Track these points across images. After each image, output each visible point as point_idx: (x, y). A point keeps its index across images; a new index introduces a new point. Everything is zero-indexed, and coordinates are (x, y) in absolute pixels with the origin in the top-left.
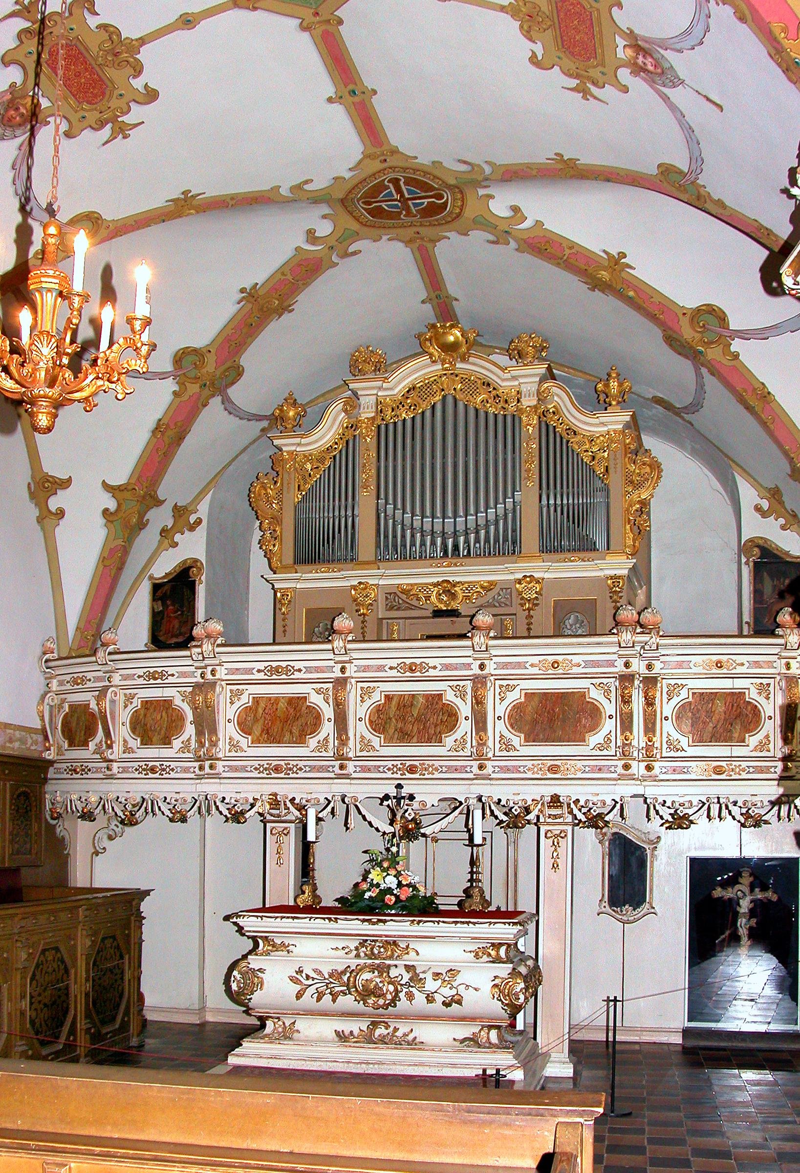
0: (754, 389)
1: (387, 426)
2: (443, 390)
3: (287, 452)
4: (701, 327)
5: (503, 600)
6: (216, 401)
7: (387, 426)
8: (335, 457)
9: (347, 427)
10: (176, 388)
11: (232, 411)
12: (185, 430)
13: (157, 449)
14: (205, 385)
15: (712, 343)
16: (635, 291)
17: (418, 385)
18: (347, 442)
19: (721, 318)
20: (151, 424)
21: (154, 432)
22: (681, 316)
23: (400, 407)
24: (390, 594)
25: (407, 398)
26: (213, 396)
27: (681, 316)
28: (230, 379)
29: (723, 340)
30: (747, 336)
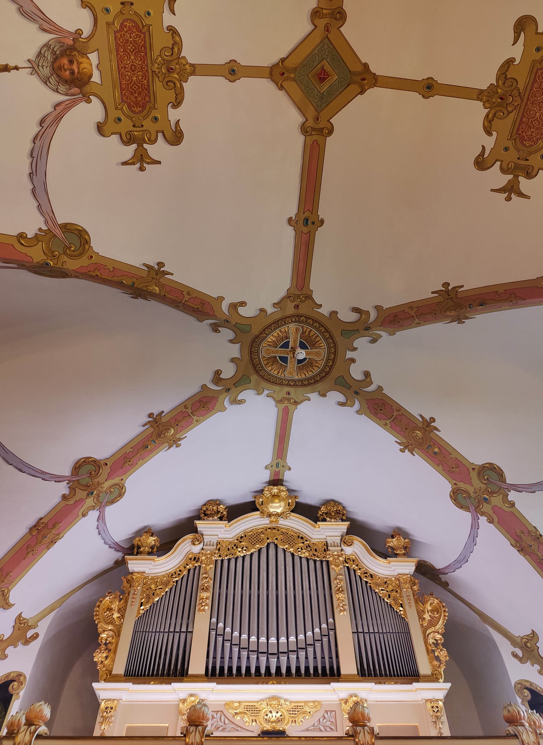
0: (529, 532)
1: (222, 561)
2: (268, 539)
3: (138, 573)
4: (485, 480)
5: (328, 724)
6: (94, 515)
7: (222, 561)
8: (177, 581)
9: (191, 559)
10: (66, 491)
11: (102, 532)
12: (59, 534)
13: (28, 546)
14: (92, 493)
15: (495, 493)
16: (439, 448)
17: (250, 534)
18: (189, 570)
19: (500, 474)
20: (31, 521)
21: (31, 529)
22: (471, 470)
23: (235, 548)
24: (217, 712)
25: (241, 542)
26: (93, 508)
27: (471, 470)
28: (113, 496)
29: (502, 491)
30: (519, 489)
